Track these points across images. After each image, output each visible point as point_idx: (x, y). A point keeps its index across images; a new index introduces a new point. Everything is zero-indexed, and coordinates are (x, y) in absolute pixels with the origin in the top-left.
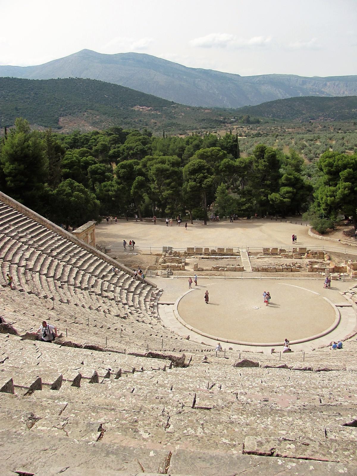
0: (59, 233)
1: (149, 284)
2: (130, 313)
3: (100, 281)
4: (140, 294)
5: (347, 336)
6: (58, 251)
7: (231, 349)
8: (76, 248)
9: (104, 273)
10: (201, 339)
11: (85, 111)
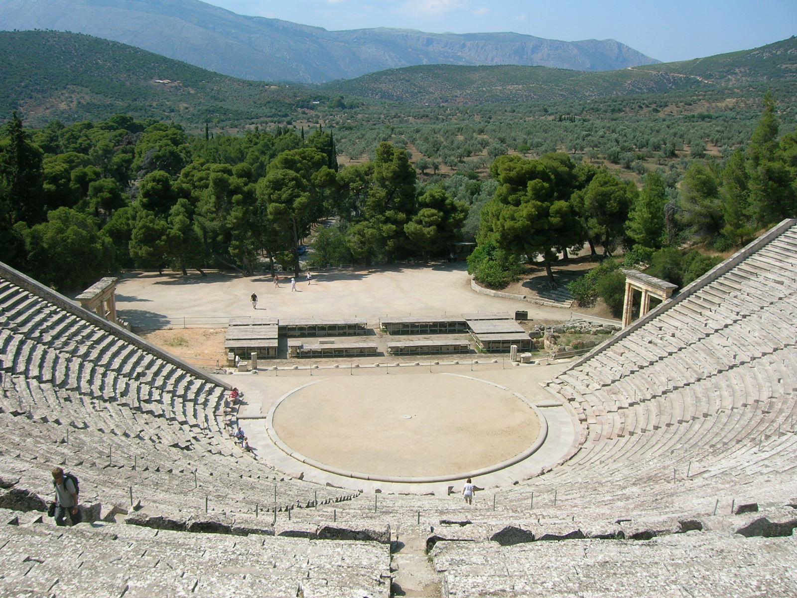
0: (51, 301)
1: (217, 385)
2: (195, 438)
3: (134, 385)
4: (205, 404)
5: (566, 455)
6: (54, 332)
7: (378, 491)
8: (84, 327)
9: (139, 369)
10: (323, 478)
11: (65, 88)
